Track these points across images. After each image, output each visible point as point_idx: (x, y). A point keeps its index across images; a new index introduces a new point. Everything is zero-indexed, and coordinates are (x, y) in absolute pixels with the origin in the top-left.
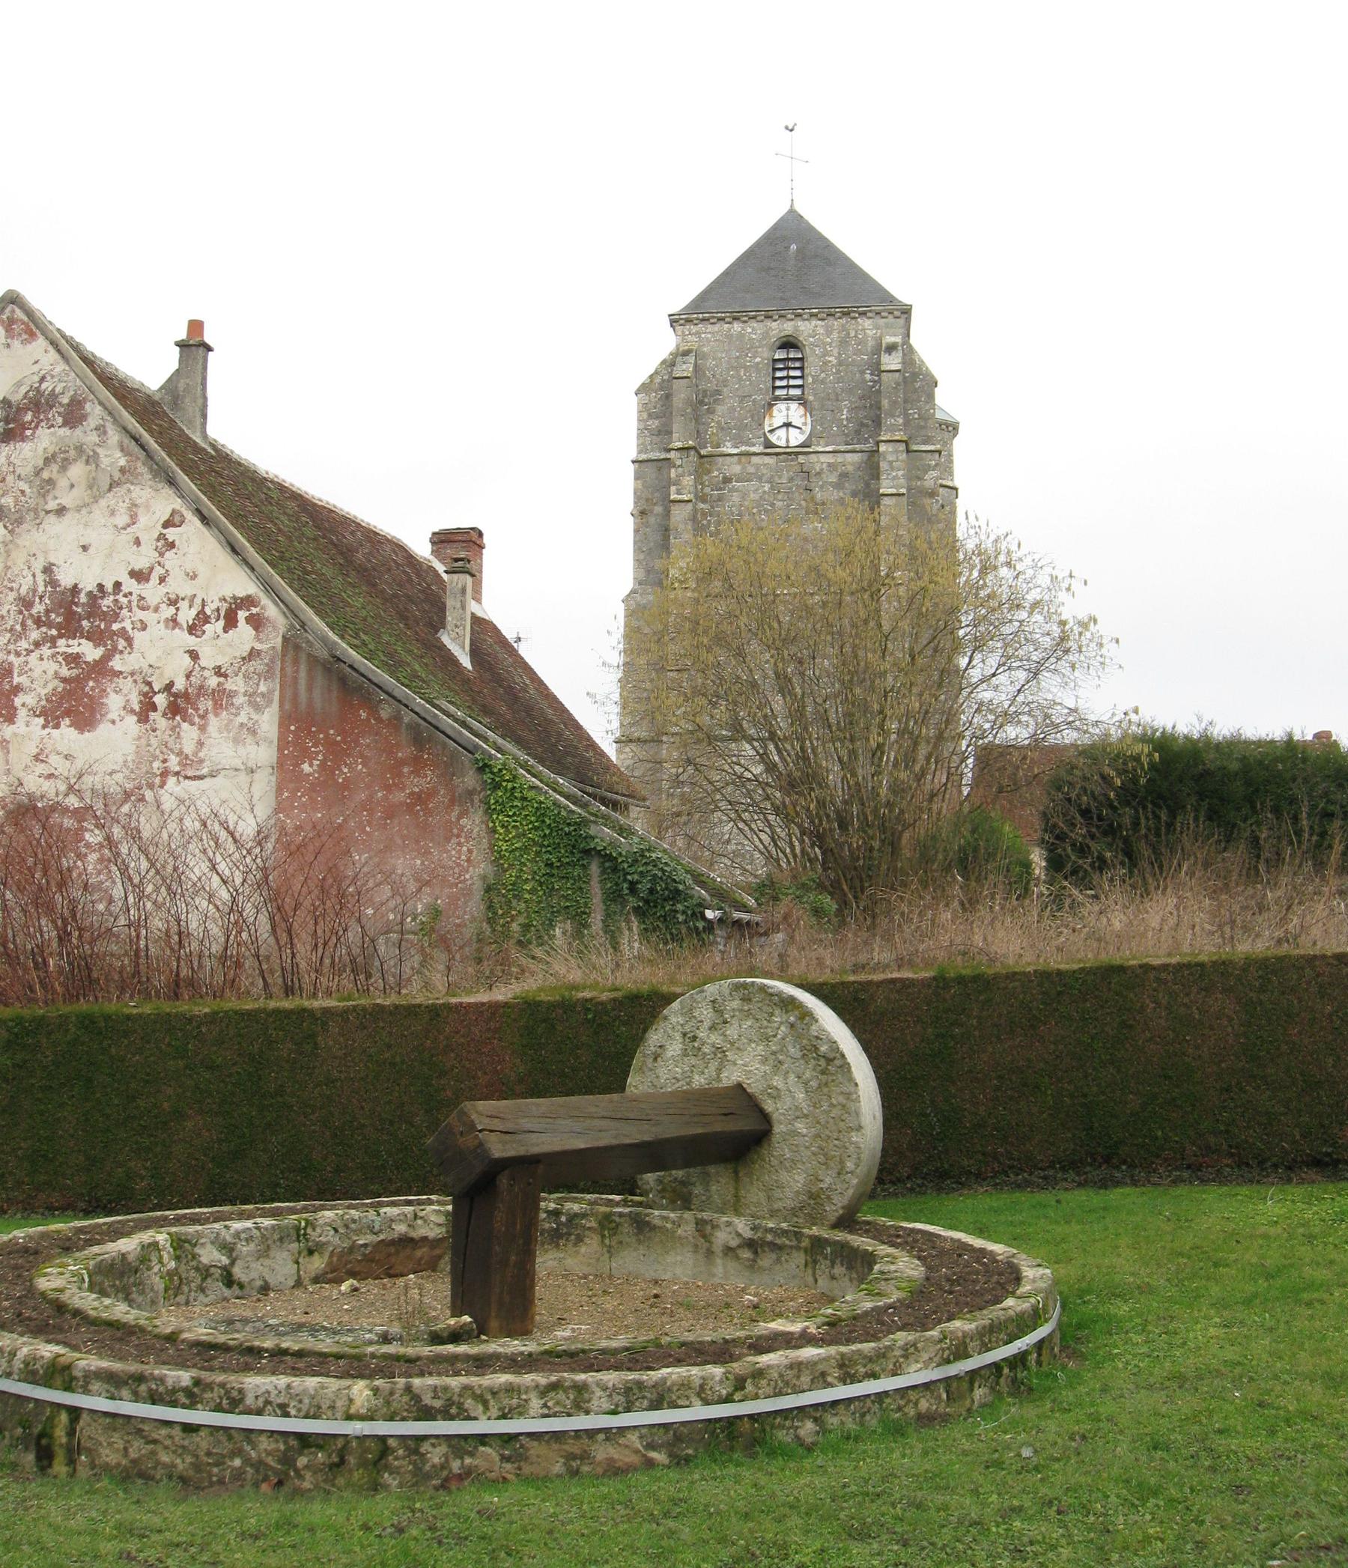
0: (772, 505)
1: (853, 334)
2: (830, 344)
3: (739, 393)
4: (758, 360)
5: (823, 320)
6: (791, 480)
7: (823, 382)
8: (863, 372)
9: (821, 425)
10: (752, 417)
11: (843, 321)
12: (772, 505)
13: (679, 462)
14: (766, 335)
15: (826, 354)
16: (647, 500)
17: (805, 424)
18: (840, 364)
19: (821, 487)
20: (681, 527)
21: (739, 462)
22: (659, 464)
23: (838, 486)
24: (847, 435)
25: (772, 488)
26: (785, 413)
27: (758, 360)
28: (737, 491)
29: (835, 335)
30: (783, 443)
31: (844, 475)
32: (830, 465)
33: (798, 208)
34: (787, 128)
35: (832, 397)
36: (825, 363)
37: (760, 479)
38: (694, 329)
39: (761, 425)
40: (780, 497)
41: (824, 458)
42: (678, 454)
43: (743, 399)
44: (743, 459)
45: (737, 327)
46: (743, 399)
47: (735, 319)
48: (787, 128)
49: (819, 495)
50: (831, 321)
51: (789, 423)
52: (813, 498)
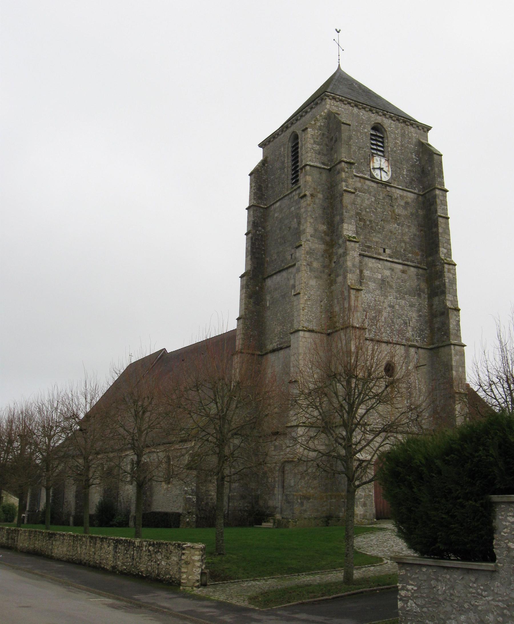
0: (376, 209)
1: (407, 133)
2: (397, 134)
3: (358, 145)
4: (366, 130)
5: (394, 121)
6: (384, 198)
7: (395, 152)
8: (411, 153)
9: (395, 174)
10: (364, 159)
11: (403, 125)
12: (376, 209)
13: (346, 170)
14: (369, 119)
15: (396, 138)
16: (314, 188)
17: (388, 171)
18: (402, 146)
19: (398, 206)
20: (349, 207)
21: (360, 182)
22: (321, 170)
23: (405, 208)
24: (406, 183)
25: (375, 200)
26: (379, 162)
27: (366, 130)
28: (359, 196)
29: (399, 130)
30: (379, 178)
31: (407, 203)
32: (401, 196)
33: (343, 68)
34: (336, 30)
35: (400, 161)
36: (396, 143)
37: (370, 193)
38: (336, 104)
39: (369, 165)
40: (379, 206)
41: (398, 191)
42: (346, 165)
43: (360, 148)
44: (362, 180)
45: (355, 110)
46: (360, 148)
47: (356, 106)
48: (336, 30)
49: (396, 210)
50: (397, 123)
51: (381, 168)
52: (394, 211)
